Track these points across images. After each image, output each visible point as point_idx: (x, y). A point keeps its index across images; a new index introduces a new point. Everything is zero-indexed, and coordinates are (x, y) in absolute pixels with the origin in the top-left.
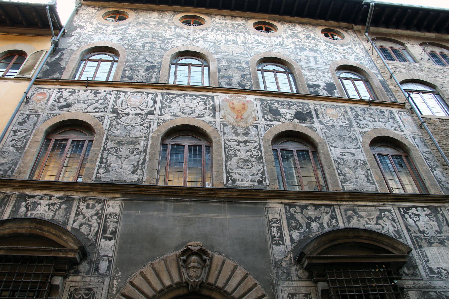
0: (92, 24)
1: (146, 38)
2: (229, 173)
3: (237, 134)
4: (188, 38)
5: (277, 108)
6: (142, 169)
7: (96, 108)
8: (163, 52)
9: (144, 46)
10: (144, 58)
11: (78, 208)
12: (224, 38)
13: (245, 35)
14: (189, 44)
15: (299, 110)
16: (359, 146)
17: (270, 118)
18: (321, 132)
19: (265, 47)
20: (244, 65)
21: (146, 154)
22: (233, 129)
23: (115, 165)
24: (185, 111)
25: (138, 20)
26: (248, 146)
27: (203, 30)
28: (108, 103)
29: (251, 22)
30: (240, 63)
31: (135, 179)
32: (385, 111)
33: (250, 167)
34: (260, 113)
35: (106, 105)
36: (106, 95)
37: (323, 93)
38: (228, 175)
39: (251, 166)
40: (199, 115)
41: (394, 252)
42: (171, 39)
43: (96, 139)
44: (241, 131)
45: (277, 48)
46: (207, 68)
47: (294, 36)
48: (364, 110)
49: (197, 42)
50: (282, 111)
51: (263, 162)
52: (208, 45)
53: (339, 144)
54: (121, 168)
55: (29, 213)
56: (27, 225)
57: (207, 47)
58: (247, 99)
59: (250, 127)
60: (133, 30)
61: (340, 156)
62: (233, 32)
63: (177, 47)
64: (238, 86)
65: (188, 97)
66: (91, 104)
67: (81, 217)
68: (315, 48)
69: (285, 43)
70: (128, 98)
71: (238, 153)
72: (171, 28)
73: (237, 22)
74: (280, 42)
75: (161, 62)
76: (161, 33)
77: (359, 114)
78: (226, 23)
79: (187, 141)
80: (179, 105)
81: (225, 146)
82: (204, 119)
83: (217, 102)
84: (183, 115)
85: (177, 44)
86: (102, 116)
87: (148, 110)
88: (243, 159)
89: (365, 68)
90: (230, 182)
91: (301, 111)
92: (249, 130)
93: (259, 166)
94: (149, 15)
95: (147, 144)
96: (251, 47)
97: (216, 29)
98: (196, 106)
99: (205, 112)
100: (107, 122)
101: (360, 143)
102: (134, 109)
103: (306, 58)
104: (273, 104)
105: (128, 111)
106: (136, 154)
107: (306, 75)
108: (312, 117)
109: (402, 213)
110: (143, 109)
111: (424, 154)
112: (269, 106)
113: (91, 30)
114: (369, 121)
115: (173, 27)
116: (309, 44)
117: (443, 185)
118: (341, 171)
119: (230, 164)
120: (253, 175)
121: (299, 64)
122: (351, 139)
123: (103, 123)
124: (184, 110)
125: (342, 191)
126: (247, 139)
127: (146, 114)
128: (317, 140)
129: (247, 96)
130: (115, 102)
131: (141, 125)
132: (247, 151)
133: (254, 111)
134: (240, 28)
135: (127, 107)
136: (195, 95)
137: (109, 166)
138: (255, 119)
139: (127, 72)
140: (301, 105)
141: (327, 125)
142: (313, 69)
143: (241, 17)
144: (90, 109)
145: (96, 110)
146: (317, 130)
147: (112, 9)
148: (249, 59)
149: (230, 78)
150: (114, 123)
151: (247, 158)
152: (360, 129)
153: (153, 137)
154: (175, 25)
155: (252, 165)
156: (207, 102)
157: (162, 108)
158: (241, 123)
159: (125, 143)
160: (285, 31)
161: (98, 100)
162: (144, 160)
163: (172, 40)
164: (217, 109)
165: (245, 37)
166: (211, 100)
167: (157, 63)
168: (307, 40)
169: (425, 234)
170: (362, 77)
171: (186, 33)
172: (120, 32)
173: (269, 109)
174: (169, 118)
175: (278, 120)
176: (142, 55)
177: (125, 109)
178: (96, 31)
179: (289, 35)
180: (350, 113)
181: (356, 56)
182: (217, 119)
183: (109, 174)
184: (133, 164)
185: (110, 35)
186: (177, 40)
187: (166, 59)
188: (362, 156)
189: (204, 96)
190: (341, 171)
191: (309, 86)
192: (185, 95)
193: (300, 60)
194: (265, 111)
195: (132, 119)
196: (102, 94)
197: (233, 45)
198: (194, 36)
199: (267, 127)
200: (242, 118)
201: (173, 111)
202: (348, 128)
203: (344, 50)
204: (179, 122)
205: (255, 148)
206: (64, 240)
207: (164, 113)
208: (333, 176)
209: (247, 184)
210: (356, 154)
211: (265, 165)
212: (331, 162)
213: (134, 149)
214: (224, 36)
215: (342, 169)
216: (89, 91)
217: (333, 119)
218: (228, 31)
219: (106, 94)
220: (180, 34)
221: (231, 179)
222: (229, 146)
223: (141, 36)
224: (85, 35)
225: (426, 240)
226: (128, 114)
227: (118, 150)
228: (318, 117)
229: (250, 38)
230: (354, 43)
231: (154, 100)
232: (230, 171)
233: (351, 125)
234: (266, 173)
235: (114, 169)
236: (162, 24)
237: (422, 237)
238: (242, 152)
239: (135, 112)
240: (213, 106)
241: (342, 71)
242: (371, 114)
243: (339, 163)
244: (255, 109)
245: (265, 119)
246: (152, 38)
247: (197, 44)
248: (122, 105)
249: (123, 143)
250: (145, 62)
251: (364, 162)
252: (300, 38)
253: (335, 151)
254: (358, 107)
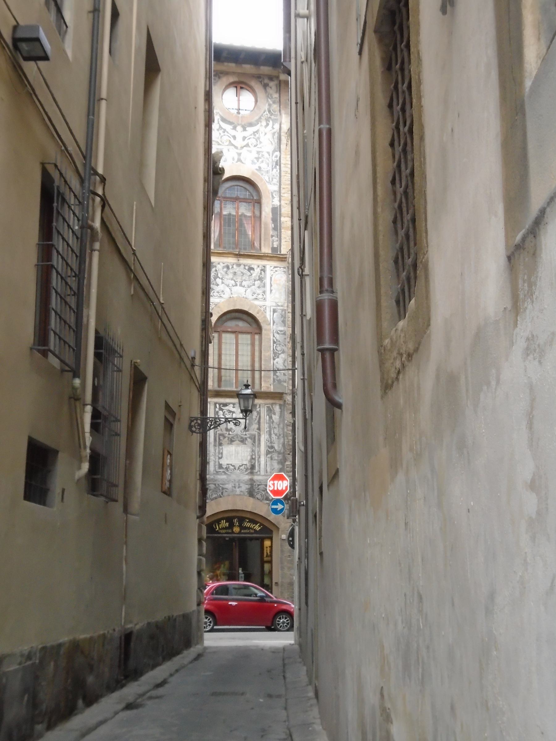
32: (255, 267)
89: (262, 180)
109: (217, 410)
111: (276, 335)
117: (277, 377)
169: (230, 433)
225: (229, 438)
237: (227, 435)
242: (235, 273)
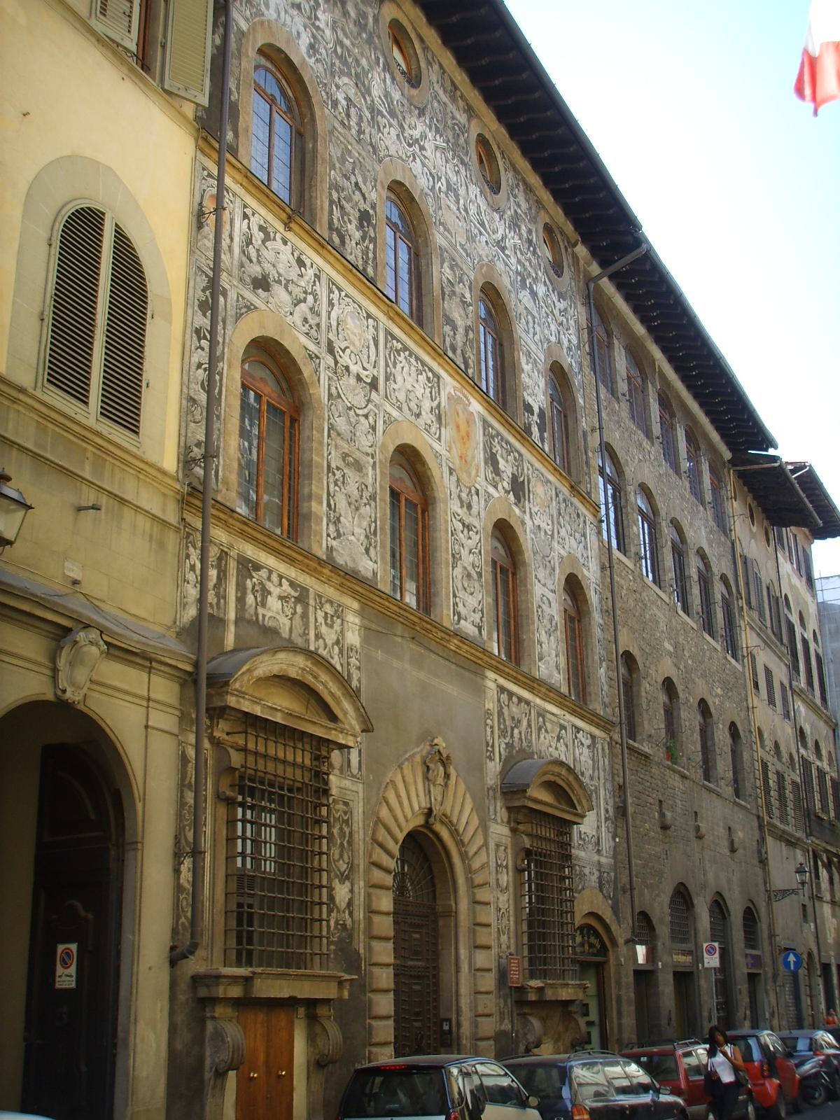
11: (316, 620)
41: (578, 808)
55: (261, 611)
56: (300, 661)
67: (321, 641)
90: (456, 618)
150: (334, 391)
153: (380, 461)
164: (443, 422)
206: (342, 710)
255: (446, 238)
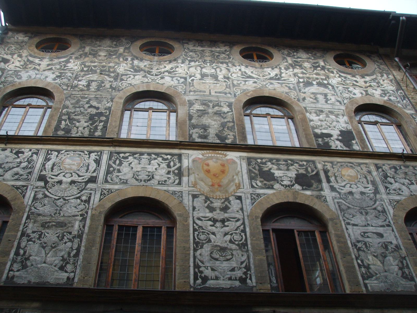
0: (20, 56)
1: (92, 74)
2: (199, 267)
3: (212, 209)
4: (149, 73)
5: (271, 169)
6: (74, 264)
7: (16, 174)
8: (114, 93)
9: (88, 86)
10: (88, 102)
12: (199, 71)
13: (228, 66)
14: (150, 80)
15: (302, 171)
16: (389, 222)
17: (260, 184)
18: (332, 202)
19: (255, 82)
20: (226, 109)
21: (81, 241)
22: (206, 202)
23: (36, 258)
24: (140, 177)
25: (83, 49)
26: (228, 226)
27: (170, 62)
28: (33, 167)
29: (237, 50)
30: (221, 106)
31: (63, 279)
33: (228, 257)
34: (246, 177)
35: (30, 170)
36: (32, 156)
37: (336, 145)
38: (196, 270)
39: (231, 257)
40: (159, 182)
42: (126, 75)
43: (13, 220)
44: (217, 204)
45: (271, 84)
46: (175, 114)
47: (296, 65)
48: (395, 168)
49: (162, 78)
50: (277, 173)
51: (247, 251)
52: (176, 82)
53: (359, 219)
54: (45, 263)
57: (174, 85)
58: (228, 157)
59: (231, 199)
60: (76, 63)
61: (360, 238)
62: (212, 62)
63: (133, 86)
64: (216, 138)
65: (146, 156)
66: (10, 169)
68: (325, 82)
69: (283, 75)
70: (62, 159)
71: (212, 237)
72: (127, 60)
73: (218, 49)
74: (276, 75)
75: (111, 107)
76: (114, 67)
77: (389, 175)
78: (203, 51)
79: (141, 221)
80: (132, 168)
81: (194, 227)
82: (165, 188)
83: (185, 163)
84: (136, 183)
85: (134, 82)
86: (24, 186)
87: (87, 176)
88: (219, 246)
89: (397, 107)
90: (199, 281)
91: (304, 172)
92: (229, 202)
93: (242, 255)
94: (98, 43)
95: (84, 227)
96: (235, 82)
97: (189, 59)
98: (156, 169)
99: (168, 178)
100: (30, 194)
101: (390, 218)
102: (69, 175)
103: (312, 96)
104: (265, 163)
105: (60, 178)
106: (67, 240)
107: (312, 121)
108: (320, 181)
110: (81, 174)
112: (259, 166)
113: (18, 64)
114: (404, 184)
115: (129, 59)
116: (317, 77)
118: (362, 261)
119: (200, 255)
120: (233, 270)
121: (303, 105)
122: (377, 212)
123: (24, 196)
124: (138, 176)
125: (365, 292)
126: (226, 215)
127: (85, 182)
128: (327, 216)
129: (228, 153)
130: (44, 165)
131: (77, 198)
132: (226, 234)
133: (237, 175)
134: (221, 56)
135: (59, 172)
136: (155, 154)
137: (28, 259)
138: (238, 187)
139: (63, 122)
140: (305, 163)
141: (342, 191)
142: (322, 111)
143: (223, 42)
144: (8, 175)
145: (16, 177)
146: (327, 200)
147: (49, 36)
148: (233, 100)
149: (205, 128)
150: (40, 196)
151: (224, 245)
152: (391, 197)
153: (93, 215)
154: (132, 55)
155: (232, 255)
156: (172, 164)
157: (108, 172)
158: (218, 193)
159: (53, 225)
160: (283, 60)
161: (21, 162)
162: (78, 249)
163: (128, 76)
164: (185, 173)
165: (229, 70)
166: (177, 160)
167: (105, 109)
168: (314, 71)
170: (393, 119)
171: (147, 66)
172: (58, 67)
173: (259, 170)
174: (116, 187)
175: (271, 187)
176: (86, 98)
177: (57, 176)
178: (25, 67)
179: (290, 64)
180: (375, 173)
181: (382, 90)
182: (184, 188)
183: (27, 271)
184: (62, 257)
185: (44, 71)
186: (134, 76)
187: (117, 103)
188: (392, 237)
189: (167, 154)
190: (362, 261)
191: (317, 136)
192: (142, 154)
193: (304, 99)
194: (253, 174)
195: (65, 189)
196: (26, 154)
197: (211, 81)
198: (158, 69)
199: (255, 198)
200: (219, 186)
201: (122, 178)
202: (372, 195)
203: (366, 82)
204: (131, 192)
205: (236, 230)
207: (110, 181)
208: (350, 269)
209: (224, 284)
210: (385, 235)
211: (251, 254)
212: (348, 248)
213: (65, 234)
214: (199, 68)
215: (363, 258)
216: (9, 150)
217: (351, 183)
218: (205, 62)
219: (32, 153)
220: (138, 67)
221: (201, 277)
222: (200, 227)
223: (85, 71)
224: (10, 72)
226: (60, 182)
227: (43, 236)
228: (329, 181)
229: (235, 71)
230: (381, 73)
231: (98, 162)
232: (200, 264)
233: (376, 192)
234: (252, 266)
235: (34, 263)
236: (114, 55)
238: (218, 236)
239: (69, 180)
240: (180, 169)
241: (364, 113)
242: (406, 173)
243: (359, 249)
244: (239, 172)
245: (253, 187)
246: (101, 74)
247: (161, 81)
248: (52, 169)
249: (51, 224)
250: (89, 107)
251: (396, 246)
252: (305, 68)
253: (353, 231)
254: (387, 164)
255: (197, 95)
